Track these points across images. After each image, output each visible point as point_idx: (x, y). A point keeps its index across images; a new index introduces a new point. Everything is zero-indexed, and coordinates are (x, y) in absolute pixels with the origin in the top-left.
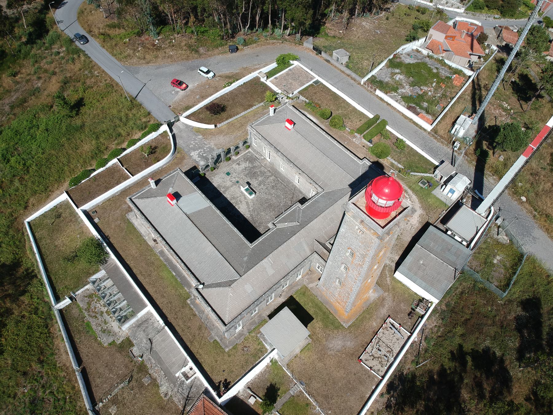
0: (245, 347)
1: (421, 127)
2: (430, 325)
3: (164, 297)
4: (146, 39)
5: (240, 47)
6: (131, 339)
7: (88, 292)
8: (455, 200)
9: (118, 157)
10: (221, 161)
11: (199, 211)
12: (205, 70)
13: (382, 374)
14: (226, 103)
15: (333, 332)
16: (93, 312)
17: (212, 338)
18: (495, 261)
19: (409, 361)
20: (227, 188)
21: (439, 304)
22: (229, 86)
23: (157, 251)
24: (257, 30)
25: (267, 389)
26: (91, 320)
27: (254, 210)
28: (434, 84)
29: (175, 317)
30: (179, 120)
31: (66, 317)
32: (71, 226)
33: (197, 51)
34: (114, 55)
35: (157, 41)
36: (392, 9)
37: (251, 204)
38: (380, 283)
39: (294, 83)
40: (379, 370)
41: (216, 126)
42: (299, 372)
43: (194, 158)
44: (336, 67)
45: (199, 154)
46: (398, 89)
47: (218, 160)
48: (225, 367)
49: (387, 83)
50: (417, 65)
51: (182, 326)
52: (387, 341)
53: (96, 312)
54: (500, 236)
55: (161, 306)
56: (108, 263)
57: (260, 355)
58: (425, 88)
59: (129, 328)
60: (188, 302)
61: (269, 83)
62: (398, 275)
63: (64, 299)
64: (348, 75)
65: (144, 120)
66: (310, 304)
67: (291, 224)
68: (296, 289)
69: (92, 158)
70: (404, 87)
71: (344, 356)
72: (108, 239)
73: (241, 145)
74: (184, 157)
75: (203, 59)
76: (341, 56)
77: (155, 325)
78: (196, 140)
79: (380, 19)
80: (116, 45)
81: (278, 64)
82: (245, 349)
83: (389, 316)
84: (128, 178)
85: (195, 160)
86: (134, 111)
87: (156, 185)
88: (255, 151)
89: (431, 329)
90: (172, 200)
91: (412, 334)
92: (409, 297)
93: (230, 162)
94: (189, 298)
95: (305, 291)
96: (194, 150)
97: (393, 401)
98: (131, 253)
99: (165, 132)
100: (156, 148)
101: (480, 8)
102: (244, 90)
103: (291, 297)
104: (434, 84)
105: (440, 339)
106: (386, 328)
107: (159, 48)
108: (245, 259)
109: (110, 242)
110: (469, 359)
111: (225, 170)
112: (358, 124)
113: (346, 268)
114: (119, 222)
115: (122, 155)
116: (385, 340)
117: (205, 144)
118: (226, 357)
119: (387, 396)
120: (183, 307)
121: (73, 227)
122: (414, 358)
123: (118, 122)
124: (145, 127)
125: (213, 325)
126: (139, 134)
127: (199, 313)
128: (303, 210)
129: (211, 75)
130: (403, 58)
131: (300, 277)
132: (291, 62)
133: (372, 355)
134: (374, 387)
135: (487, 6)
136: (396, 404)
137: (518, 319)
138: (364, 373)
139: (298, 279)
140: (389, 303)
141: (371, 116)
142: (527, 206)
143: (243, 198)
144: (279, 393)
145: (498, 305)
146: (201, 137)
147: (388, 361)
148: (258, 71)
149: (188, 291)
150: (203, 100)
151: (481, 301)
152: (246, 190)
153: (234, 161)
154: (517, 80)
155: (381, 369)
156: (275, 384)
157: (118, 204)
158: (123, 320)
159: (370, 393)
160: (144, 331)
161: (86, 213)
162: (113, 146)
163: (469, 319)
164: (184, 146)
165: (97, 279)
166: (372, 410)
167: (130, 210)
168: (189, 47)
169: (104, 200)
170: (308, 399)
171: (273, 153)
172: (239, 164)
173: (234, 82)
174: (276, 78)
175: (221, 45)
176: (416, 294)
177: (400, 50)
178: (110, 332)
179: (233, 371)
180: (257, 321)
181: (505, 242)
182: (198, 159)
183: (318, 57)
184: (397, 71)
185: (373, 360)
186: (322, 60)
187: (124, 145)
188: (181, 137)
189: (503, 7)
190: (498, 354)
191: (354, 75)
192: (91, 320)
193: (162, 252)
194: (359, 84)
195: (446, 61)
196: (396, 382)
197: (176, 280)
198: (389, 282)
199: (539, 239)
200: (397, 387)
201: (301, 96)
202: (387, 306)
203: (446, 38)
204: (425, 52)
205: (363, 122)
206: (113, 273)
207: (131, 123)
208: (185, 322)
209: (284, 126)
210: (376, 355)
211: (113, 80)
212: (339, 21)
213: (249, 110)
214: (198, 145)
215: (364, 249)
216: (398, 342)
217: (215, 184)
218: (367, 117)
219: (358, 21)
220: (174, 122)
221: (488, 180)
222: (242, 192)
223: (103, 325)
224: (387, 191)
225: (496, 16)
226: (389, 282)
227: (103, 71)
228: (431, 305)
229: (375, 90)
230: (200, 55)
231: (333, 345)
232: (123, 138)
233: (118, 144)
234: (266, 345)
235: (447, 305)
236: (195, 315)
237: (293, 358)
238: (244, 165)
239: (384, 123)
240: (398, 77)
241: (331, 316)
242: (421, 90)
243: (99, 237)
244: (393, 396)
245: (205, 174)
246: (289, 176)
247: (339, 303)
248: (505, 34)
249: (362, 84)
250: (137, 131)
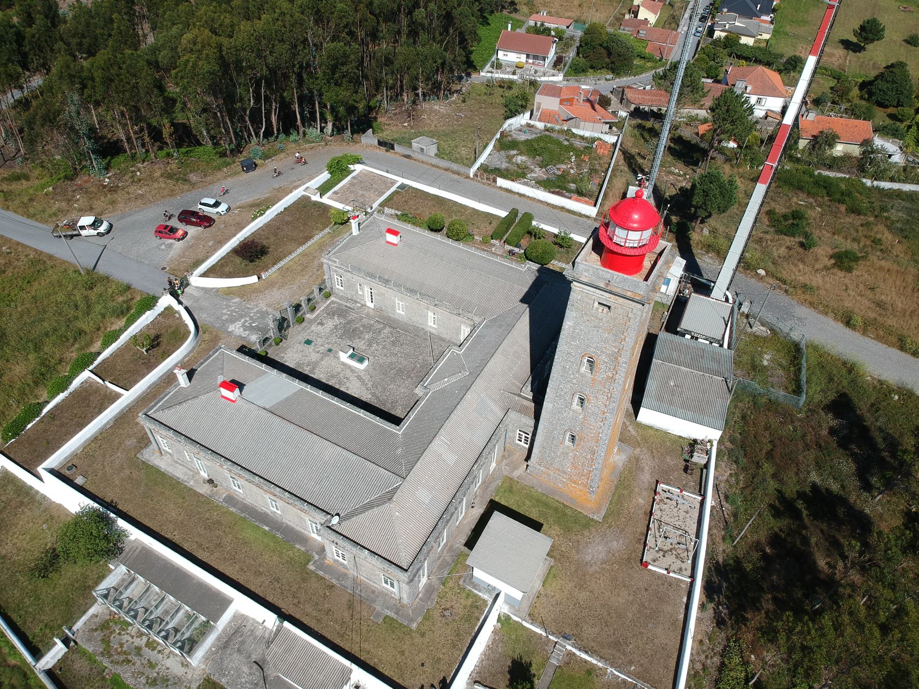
0: (445, 609)
1: (580, 215)
2: (723, 475)
3: (261, 574)
4: (86, 182)
5: (258, 161)
6: (214, 678)
7: (97, 620)
8: (673, 294)
9: (91, 367)
10: (288, 326)
11: (286, 400)
12: (212, 201)
13: (689, 572)
14: (265, 243)
15: (582, 535)
16: (119, 654)
17: (378, 615)
18: (765, 363)
19: (718, 539)
20: (315, 365)
21: (720, 442)
22: (261, 215)
23: (220, 498)
24: (277, 137)
25: (509, 672)
26: (118, 670)
27: (375, 386)
28: (573, 159)
29: (295, 601)
30: (188, 284)
31: (63, 681)
32: (23, 513)
33: (186, 180)
34: (31, 216)
35: (107, 180)
36: (464, 89)
37: (366, 378)
38: (624, 439)
39: (367, 194)
40: (681, 569)
42: (554, 620)
43: (238, 334)
44: (423, 162)
45: (243, 325)
46: (526, 174)
47: (282, 324)
48: (422, 656)
49: (507, 170)
50: (539, 140)
51: (315, 613)
52: (672, 520)
53: (125, 653)
54: (754, 329)
55: (259, 591)
56: (127, 550)
57: (476, 614)
58: (563, 167)
59: (206, 658)
60: (311, 567)
61: (325, 200)
62: (646, 416)
63: (55, 644)
64: (447, 170)
65: (121, 299)
66: (527, 502)
67: (454, 379)
68: (493, 487)
69: (36, 383)
70: (532, 171)
71: (616, 566)
72: (115, 507)
73: (316, 291)
74: (216, 336)
75: (200, 190)
76: (425, 147)
77: (259, 633)
78: (231, 307)
79: (454, 102)
80: (31, 200)
81: (331, 173)
82: (447, 613)
83: (657, 482)
84: (118, 396)
85: (240, 336)
86: (98, 289)
87: (190, 380)
88: (341, 298)
89: (727, 481)
90: (232, 391)
91: (704, 497)
92: (672, 444)
93: (304, 324)
94: (309, 561)
95: (510, 485)
96: (232, 321)
97: (725, 611)
98: (169, 515)
99: (169, 309)
100: (157, 337)
101: (583, 71)
102: (288, 218)
103: (492, 501)
104: (573, 159)
105: (747, 492)
106: (661, 500)
107: (113, 189)
108: (399, 451)
109: (118, 509)
110: (800, 505)
111: (300, 338)
112: (490, 230)
113: (582, 400)
114: (127, 472)
115: (96, 363)
116: (668, 520)
117: (248, 308)
118: (418, 640)
119: (711, 606)
120: (304, 580)
121: (28, 513)
122: (723, 533)
123: (72, 313)
124: (129, 309)
125: (373, 592)
126: (122, 322)
127: (338, 580)
128: (464, 354)
129: (223, 208)
130: (515, 136)
131: (494, 465)
132: (352, 167)
133: (660, 550)
134: (685, 600)
135: (592, 67)
136: (731, 614)
137: (832, 431)
138: (660, 582)
139: (492, 469)
140: (648, 463)
141: (503, 214)
142: (771, 280)
143: (348, 372)
144: (533, 670)
145: (800, 420)
146: (237, 300)
147: (687, 550)
148: (304, 187)
149: (303, 549)
150: (222, 246)
151: (775, 421)
152: (352, 357)
153: (311, 322)
154: (672, 145)
155: (684, 566)
156: (521, 658)
157: (116, 443)
158: (189, 646)
159: (682, 611)
160: (239, 650)
161: (52, 472)
162: (73, 355)
163: (772, 450)
164: (211, 320)
165: (108, 590)
166: (699, 637)
167: (144, 441)
168: (170, 176)
169: (85, 442)
170: (586, 661)
171: (381, 288)
172: (321, 324)
173: (268, 208)
174: (335, 193)
175: (227, 165)
176: (680, 437)
177: (506, 126)
178: (168, 680)
179: (439, 659)
180: (449, 559)
181: (765, 334)
182: (245, 334)
183: (390, 154)
184: (515, 152)
185: (664, 556)
186: (398, 157)
187: (94, 349)
188: (202, 309)
189: (613, 63)
190: (835, 487)
191: (455, 167)
192: (118, 670)
193: (231, 499)
194: (468, 177)
195: (574, 131)
196: (715, 579)
197: (274, 537)
198: (633, 433)
199: (806, 318)
200: (720, 587)
201: (386, 209)
202: (647, 468)
203: (561, 103)
204: (540, 125)
205: (495, 224)
206: (145, 564)
207: (98, 308)
208: (317, 604)
209: (384, 242)
210: (665, 548)
211: (42, 253)
212: (398, 111)
213: (310, 243)
214: (236, 312)
215: (615, 341)
216: (688, 516)
217: (292, 366)
218: (498, 217)
219: (425, 105)
221: (705, 261)
222: (343, 364)
223: (148, 671)
224: (636, 217)
225: (608, 77)
226: (633, 433)
227: (18, 244)
228: (712, 445)
229: (495, 181)
230: (193, 185)
231: (590, 556)
232: (88, 337)
233: (82, 348)
234: (480, 594)
235: (732, 441)
236: (332, 587)
237: (536, 600)
238: (330, 324)
239: (528, 217)
240: (520, 159)
241: (568, 511)
242: (559, 169)
243: (96, 505)
244: (719, 603)
245: (267, 353)
246: (414, 319)
247: (575, 482)
248: (629, 94)
249: (471, 176)
250: (113, 320)
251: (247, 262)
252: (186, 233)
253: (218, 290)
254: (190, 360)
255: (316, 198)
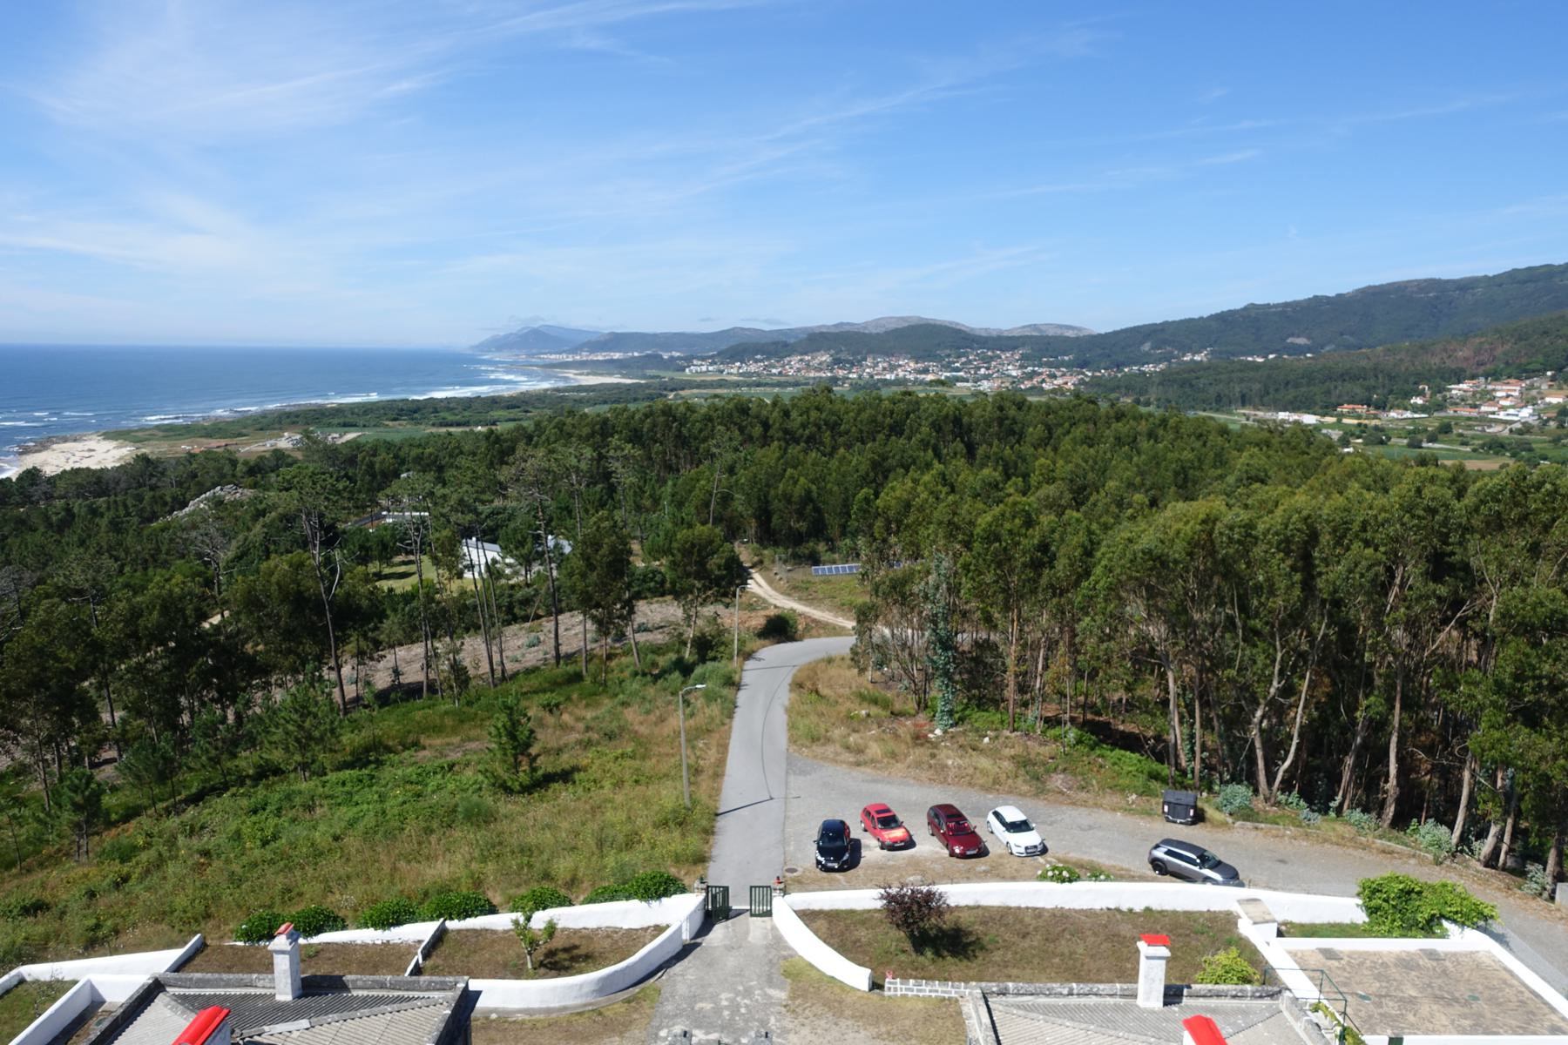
12: (1013, 814)
41: (876, 986)
168: (1024, 763)
174: (1329, 954)
220: (740, 913)
251: (908, 946)
252: (909, 843)
253: (791, 955)
254: (523, 1022)
255: (1261, 937)
